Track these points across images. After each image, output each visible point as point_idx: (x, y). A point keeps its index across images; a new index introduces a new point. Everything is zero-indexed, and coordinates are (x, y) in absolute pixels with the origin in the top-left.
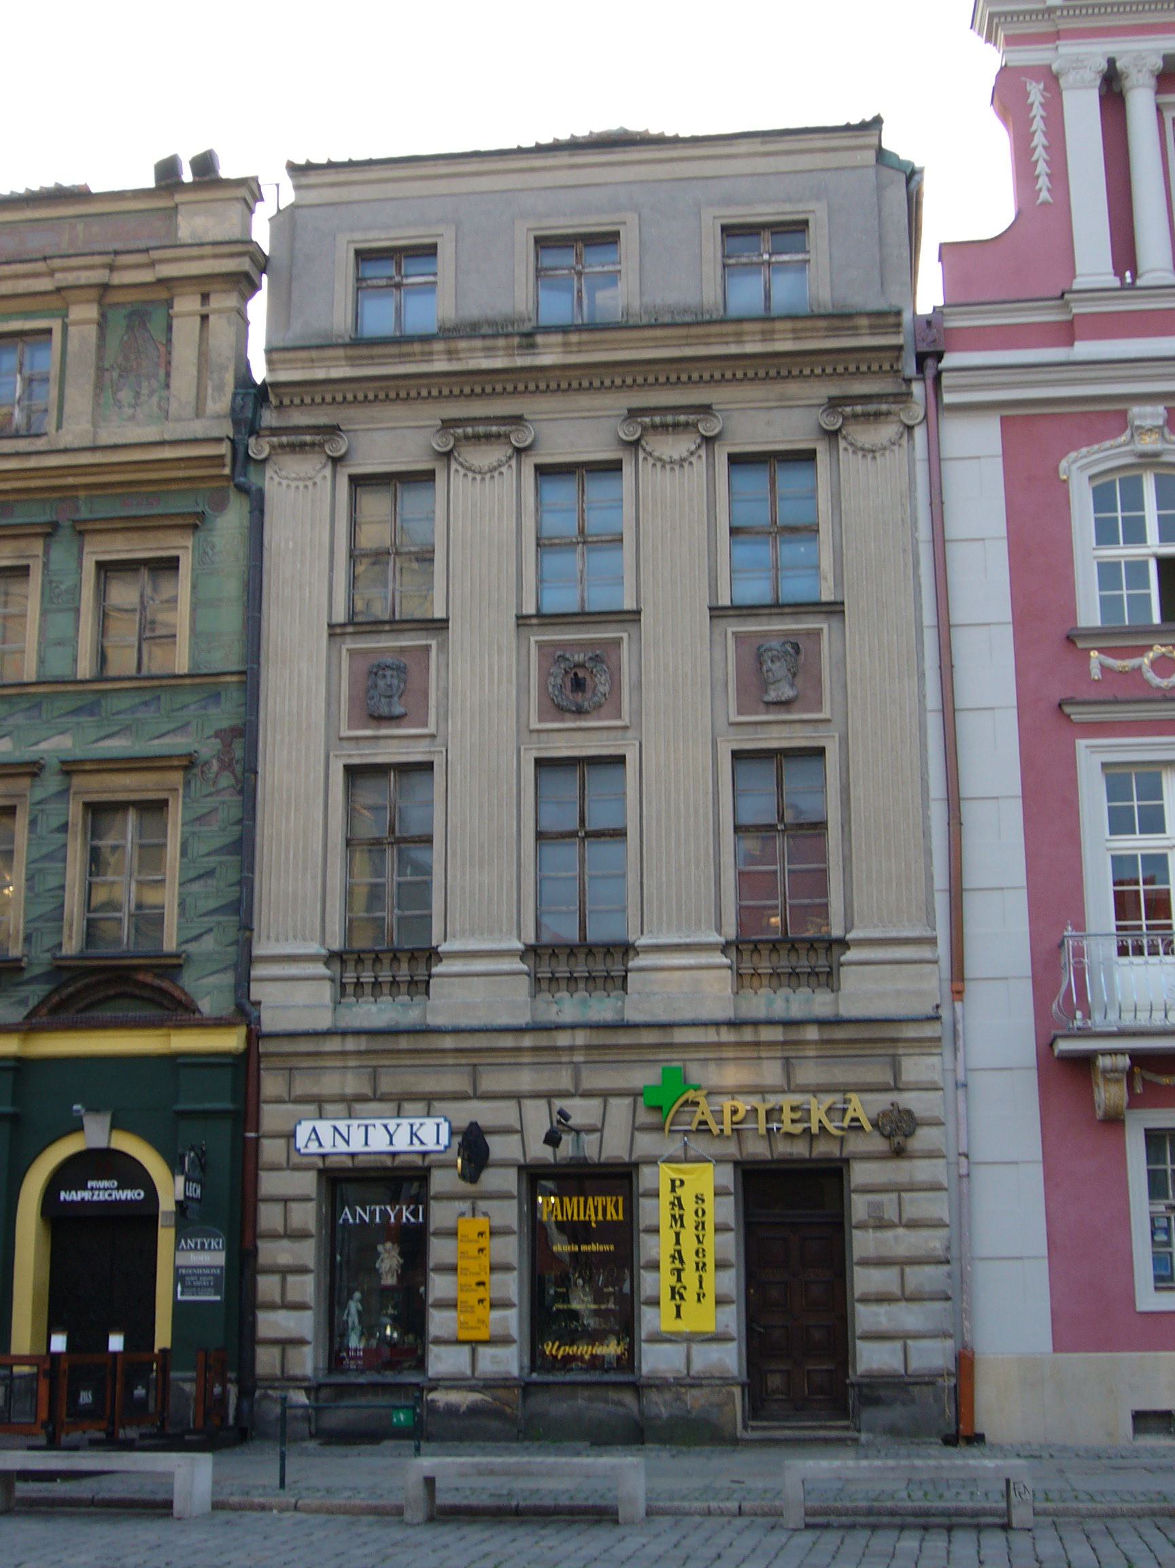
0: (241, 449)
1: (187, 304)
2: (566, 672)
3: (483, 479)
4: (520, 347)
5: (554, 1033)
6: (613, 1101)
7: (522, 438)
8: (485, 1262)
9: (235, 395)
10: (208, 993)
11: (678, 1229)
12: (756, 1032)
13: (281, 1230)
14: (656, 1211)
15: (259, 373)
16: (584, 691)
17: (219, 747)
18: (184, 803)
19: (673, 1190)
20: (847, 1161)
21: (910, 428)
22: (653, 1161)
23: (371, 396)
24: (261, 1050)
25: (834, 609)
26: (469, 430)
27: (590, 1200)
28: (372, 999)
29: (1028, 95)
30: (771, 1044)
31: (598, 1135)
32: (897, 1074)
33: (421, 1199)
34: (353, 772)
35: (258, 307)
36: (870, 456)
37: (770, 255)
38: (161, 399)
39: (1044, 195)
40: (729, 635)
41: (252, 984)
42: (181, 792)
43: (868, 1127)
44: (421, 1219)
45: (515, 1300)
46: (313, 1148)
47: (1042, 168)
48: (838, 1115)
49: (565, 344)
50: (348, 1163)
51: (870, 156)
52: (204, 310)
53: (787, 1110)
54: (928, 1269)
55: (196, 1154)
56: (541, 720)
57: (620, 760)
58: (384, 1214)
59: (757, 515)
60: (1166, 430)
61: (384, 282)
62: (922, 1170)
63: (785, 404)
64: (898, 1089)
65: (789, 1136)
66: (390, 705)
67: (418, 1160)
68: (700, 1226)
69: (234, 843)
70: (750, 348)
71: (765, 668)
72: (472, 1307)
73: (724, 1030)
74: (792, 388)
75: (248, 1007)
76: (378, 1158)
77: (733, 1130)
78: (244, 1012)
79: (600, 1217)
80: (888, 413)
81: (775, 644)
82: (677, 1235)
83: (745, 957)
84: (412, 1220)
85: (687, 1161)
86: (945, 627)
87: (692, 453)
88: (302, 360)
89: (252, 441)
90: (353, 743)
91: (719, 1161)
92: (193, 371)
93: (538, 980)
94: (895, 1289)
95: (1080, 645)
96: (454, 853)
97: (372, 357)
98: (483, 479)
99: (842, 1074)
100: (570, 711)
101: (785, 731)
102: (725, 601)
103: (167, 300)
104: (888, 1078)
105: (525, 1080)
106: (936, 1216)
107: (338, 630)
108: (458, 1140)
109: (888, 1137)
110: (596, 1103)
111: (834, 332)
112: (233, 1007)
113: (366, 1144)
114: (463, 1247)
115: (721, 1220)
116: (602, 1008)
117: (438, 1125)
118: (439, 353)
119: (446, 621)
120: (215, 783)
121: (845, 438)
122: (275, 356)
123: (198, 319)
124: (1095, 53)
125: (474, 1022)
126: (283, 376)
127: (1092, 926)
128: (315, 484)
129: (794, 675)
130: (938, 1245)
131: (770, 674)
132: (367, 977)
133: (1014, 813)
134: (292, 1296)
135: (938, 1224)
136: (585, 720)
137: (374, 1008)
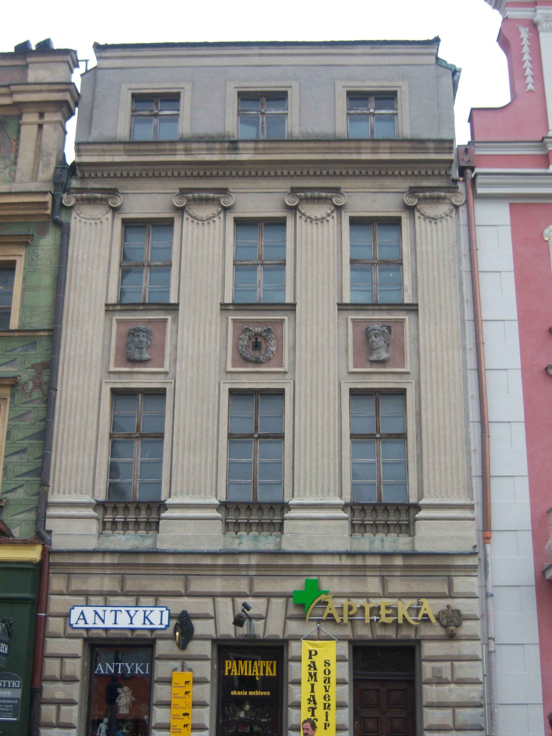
0: (58, 200)
1: (30, 118)
2: (250, 338)
3: (203, 224)
4: (229, 149)
5: (237, 556)
6: (273, 600)
7: (226, 202)
8: (189, 700)
9: (56, 168)
10: (19, 525)
11: (313, 682)
12: (364, 559)
13: (58, 676)
14: (300, 670)
15: (71, 157)
16: (260, 350)
17: (34, 374)
18: (10, 407)
19: (310, 657)
21: (457, 207)
22: (298, 639)
23: (138, 174)
24: (51, 561)
25: (413, 308)
26: (196, 195)
27: (255, 662)
28: (122, 532)
29: (520, 34)
31: (263, 621)
33: (151, 659)
34: (116, 393)
35: (72, 125)
36: (433, 222)
37: (375, 109)
38: (11, 170)
39: (530, 87)
40: (349, 321)
41: (47, 520)
42: (9, 400)
43: (433, 620)
44: (147, 673)
45: (208, 725)
46: (81, 624)
48: (414, 612)
49: (256, 149)
50: (103, 634)
51: (432, 60)
52: (41, 121)
54: (470, 711)
55: (6, 625)
56: (233, 366)
57: (281, 393)
58: (124, 669)
59: (366, 254)
61: (147, 113)
62: (466, 648)
63: (384, 191)
64: (451, 596)
65: (384, 625)
66: (141, 353)
67: (148, 634)
68: (327, 680)
69: (39, 433)
71: (370, 340)
72: (180, 729)
73: (344, 558)
74: (388, 182)
75: (44, 533)
76: (122, 632)
77: (349, 620)
78: (41, 536)
79: (262, 674)
80: (444, 198)
81: (377, 326)
82: (313, 686)
83: (356, 514)
84: (142, 672)
85: (319, 639)
86: (476, 320)
87: (329, 215)
88: (98, 151)
89: (65, 195)
90: (116, 376)
91: (340, 639)
92: (31, 156)
93: (227, 524)
94: (450, 723)
96: (178, 444)
97: (140, 151)
98: (203, 224)
99: (417, 586)
100: (251, 361)
101: (382, 378)
102: (347, 299)
103: (18, 116)
104: (446, 590)
105: (218, 585)
106: (474, 677)
107: (111, 308)
108: (174, 622)
109: (445, 627)
110: (263, 601)
111: (413, 150)
112: (34, 534)
113: (115, 623)
114: (175, 690)
115: (340, 677)
116: (267, 542)
117: (162, 612)
118: (180, 150)
119: (177, 305)
120: (30, 396)
121: (419, 211)
122: (82, 147)
123: (36, 127)
125: (187, 548)
126: (86, 159)
128: (101, 222)
130: (476, 695)
131: (374, 344)
132: (120, 518)
133: (520, 431)
134: (64, 719)
135: (476, 682)
136: (260, 367)
137: (123, 538)
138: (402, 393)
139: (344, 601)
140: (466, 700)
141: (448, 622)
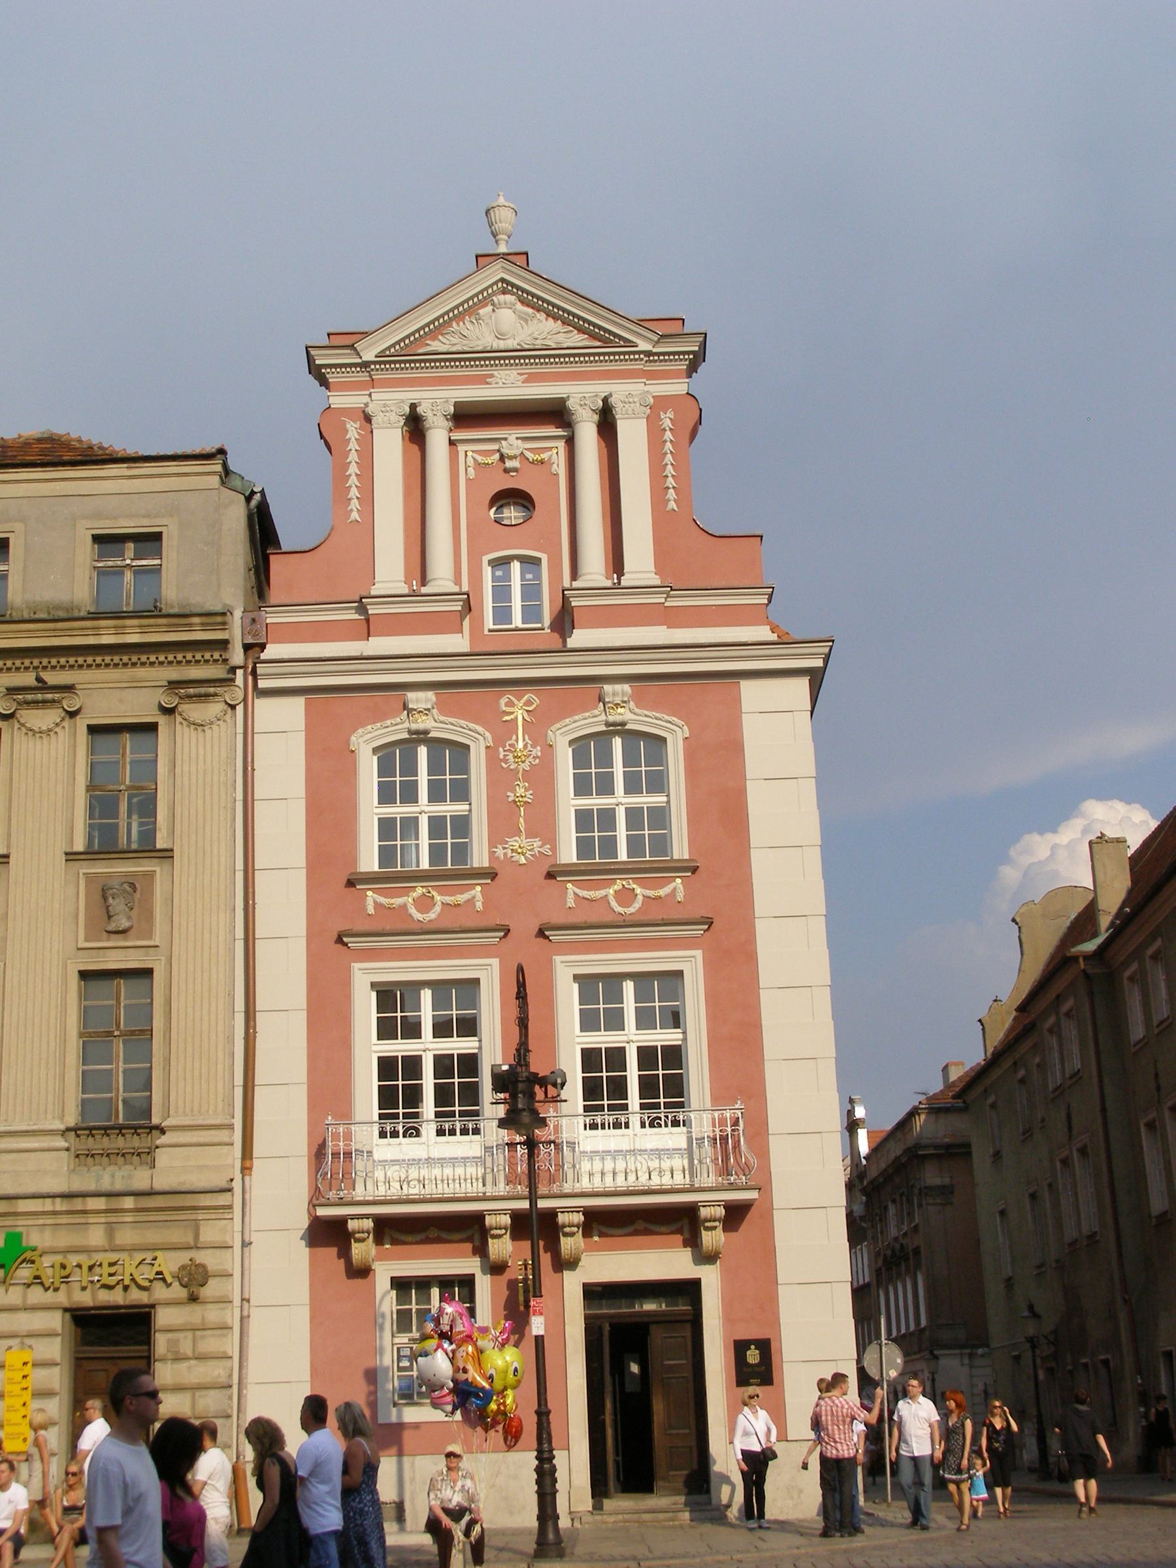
20: (153, 1306)
21: (233, 707)
29: (347, 431)
32: (197, 1236)
36: (200, 729)
39: (355, 515)
53: (105, 1265)
60: (435, 711)
62: (212, 1314)
63: (135, 685)
80: (216, 695)
101: (119, 954)
104: (190, 1239)
127: (359, 1115)
138: (148, 973)
139: (59, 1259)
140: (209, 1379)
141: (190, 1280)
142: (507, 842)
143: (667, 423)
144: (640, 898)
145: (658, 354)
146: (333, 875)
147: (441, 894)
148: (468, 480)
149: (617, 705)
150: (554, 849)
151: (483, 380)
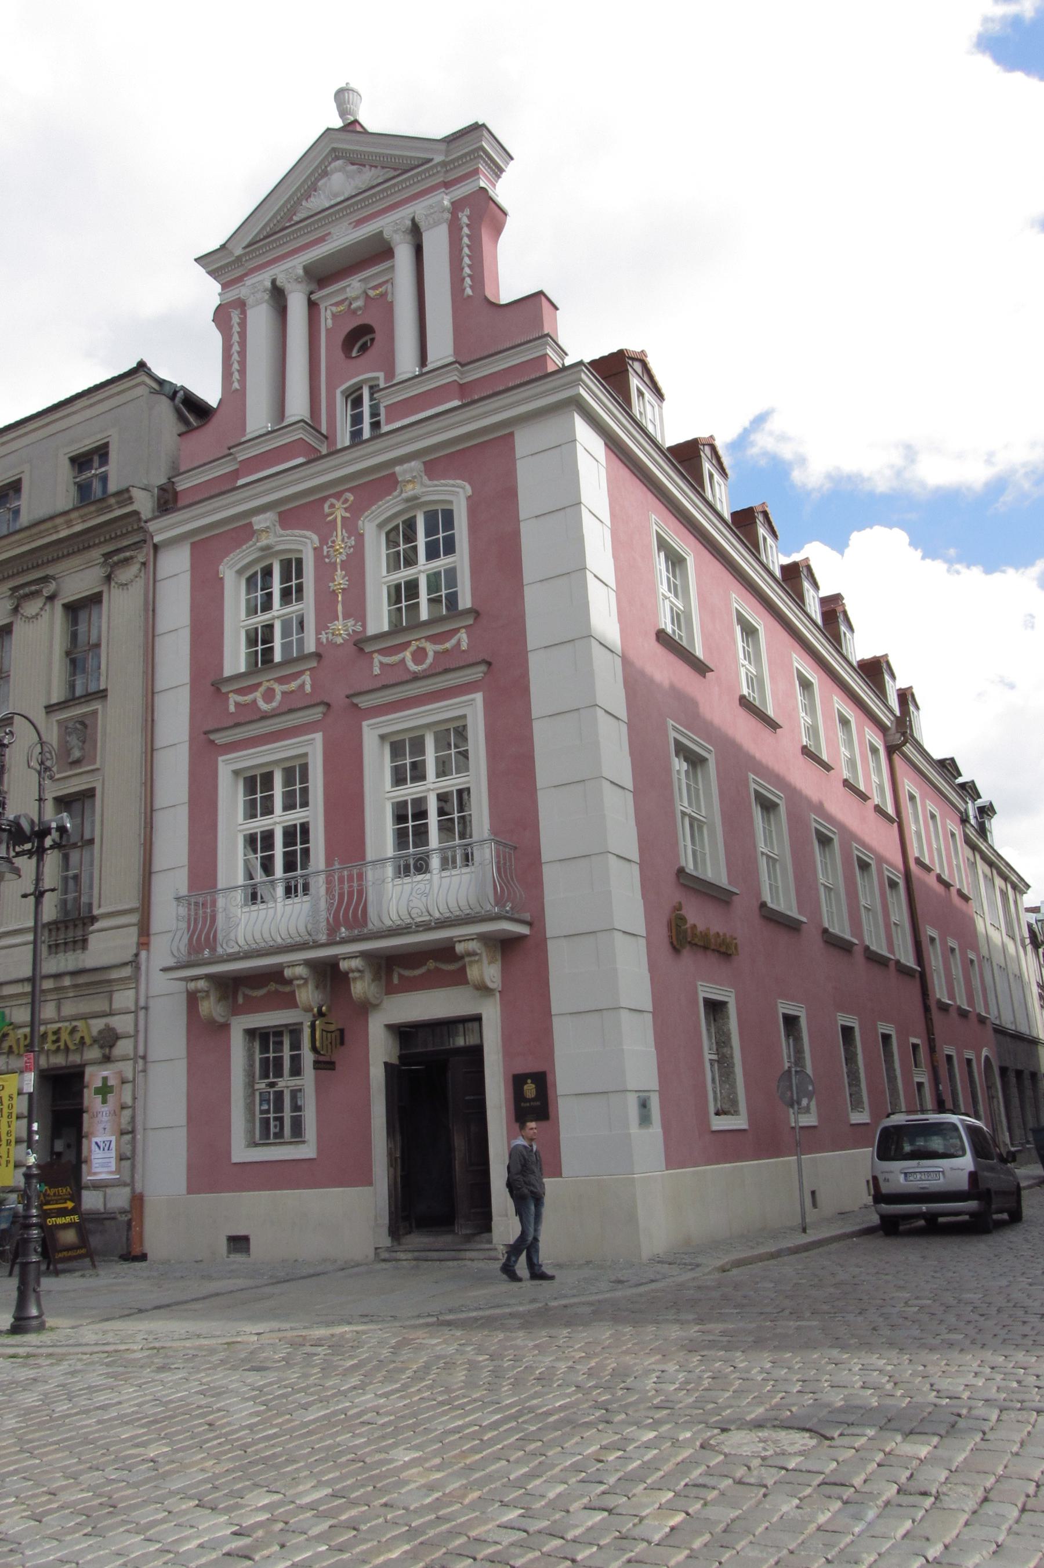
29: (230, 319)
30: (50, 991)
39: (236, 385)
47: (236, 366)
64: (111, 1014)
70: (63, 534)
80: (132, 558)
85: (8, 1073)
95: (224, 690)
109: (101, 1047)
124: (264, 278)
129: (84, 742)
142: (328, 628)
143: (465, 220)
144: (431, 654)
145: (453, 161)
146: (209, 684)
147: (281, 684)
148: (327, 330)
149: (408, 482)
150: (364, 626)
151: (321, 240)
